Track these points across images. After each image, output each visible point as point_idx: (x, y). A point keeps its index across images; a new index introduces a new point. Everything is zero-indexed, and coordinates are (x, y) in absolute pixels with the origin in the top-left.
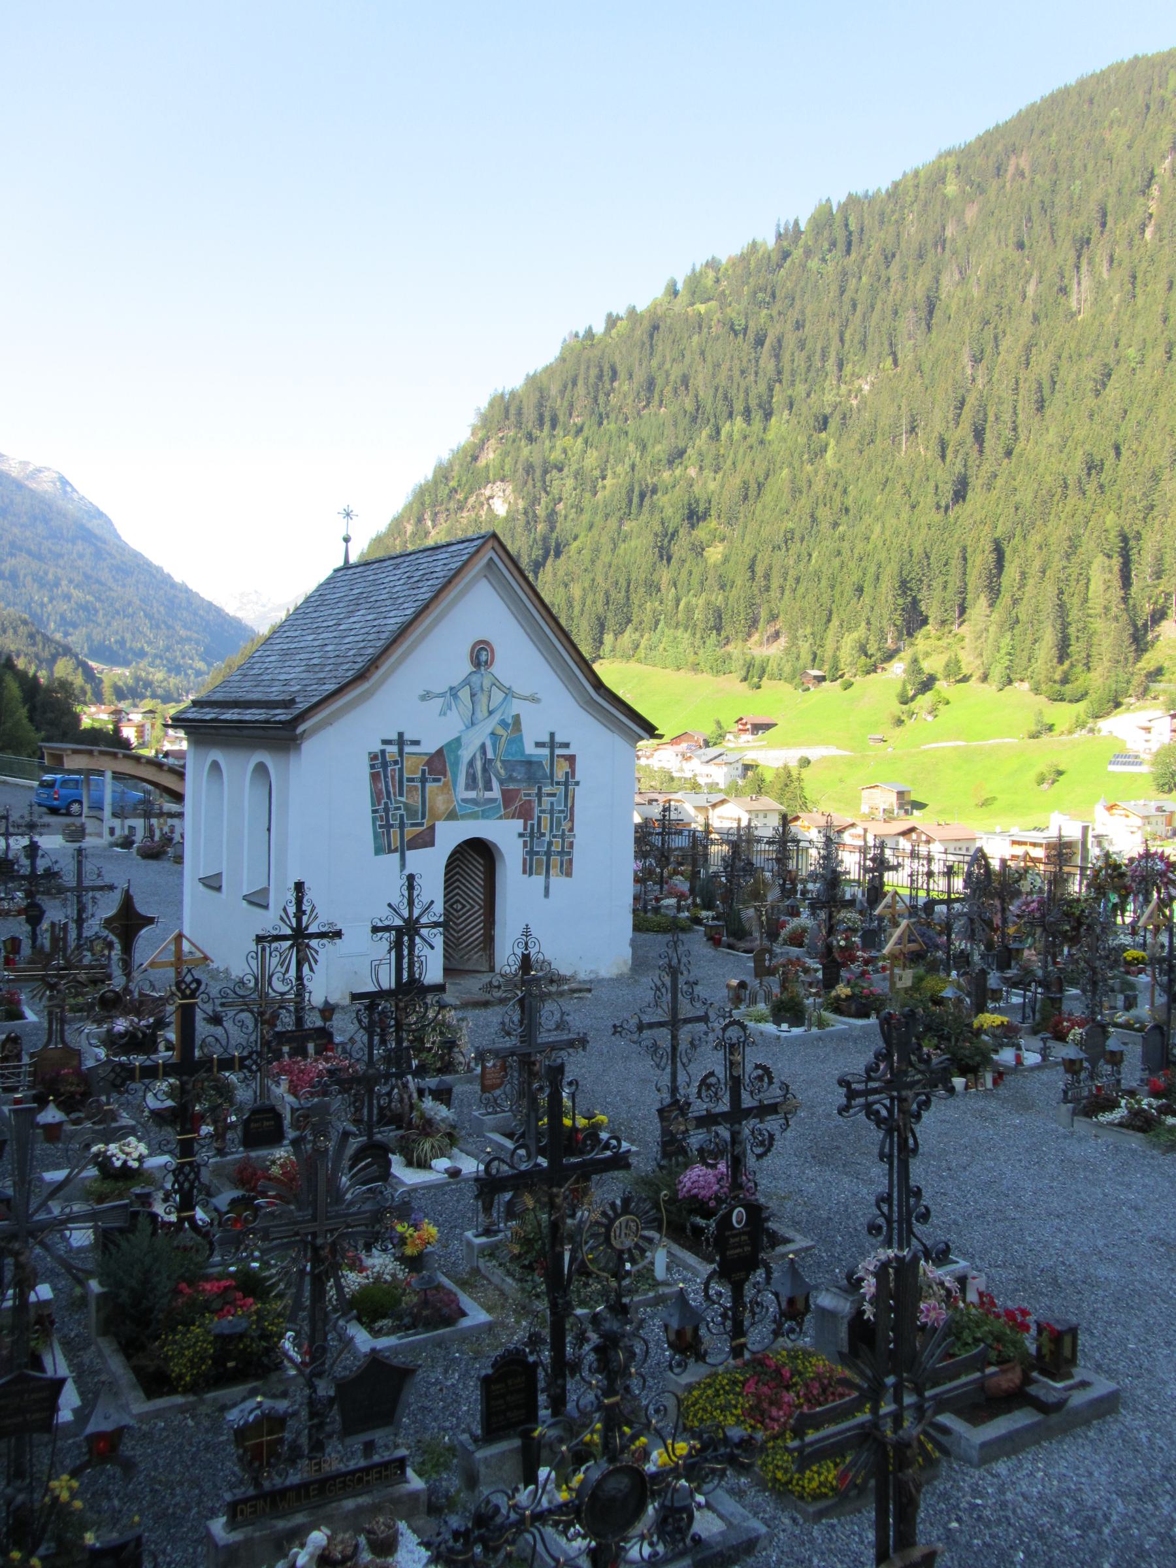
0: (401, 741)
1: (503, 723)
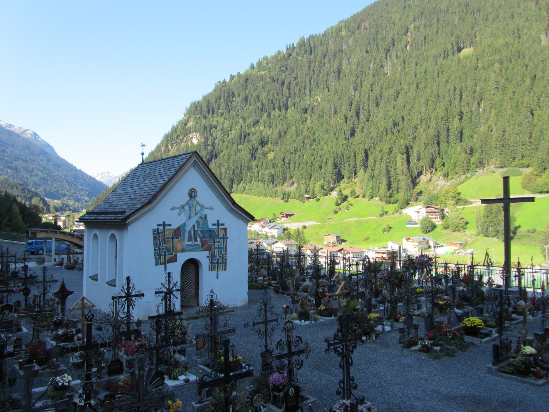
0: (164, 225)
1: (201, 217)
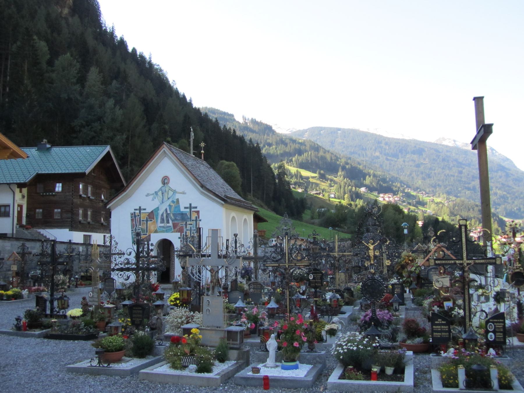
0: (140, 209)
1: (173, 202)
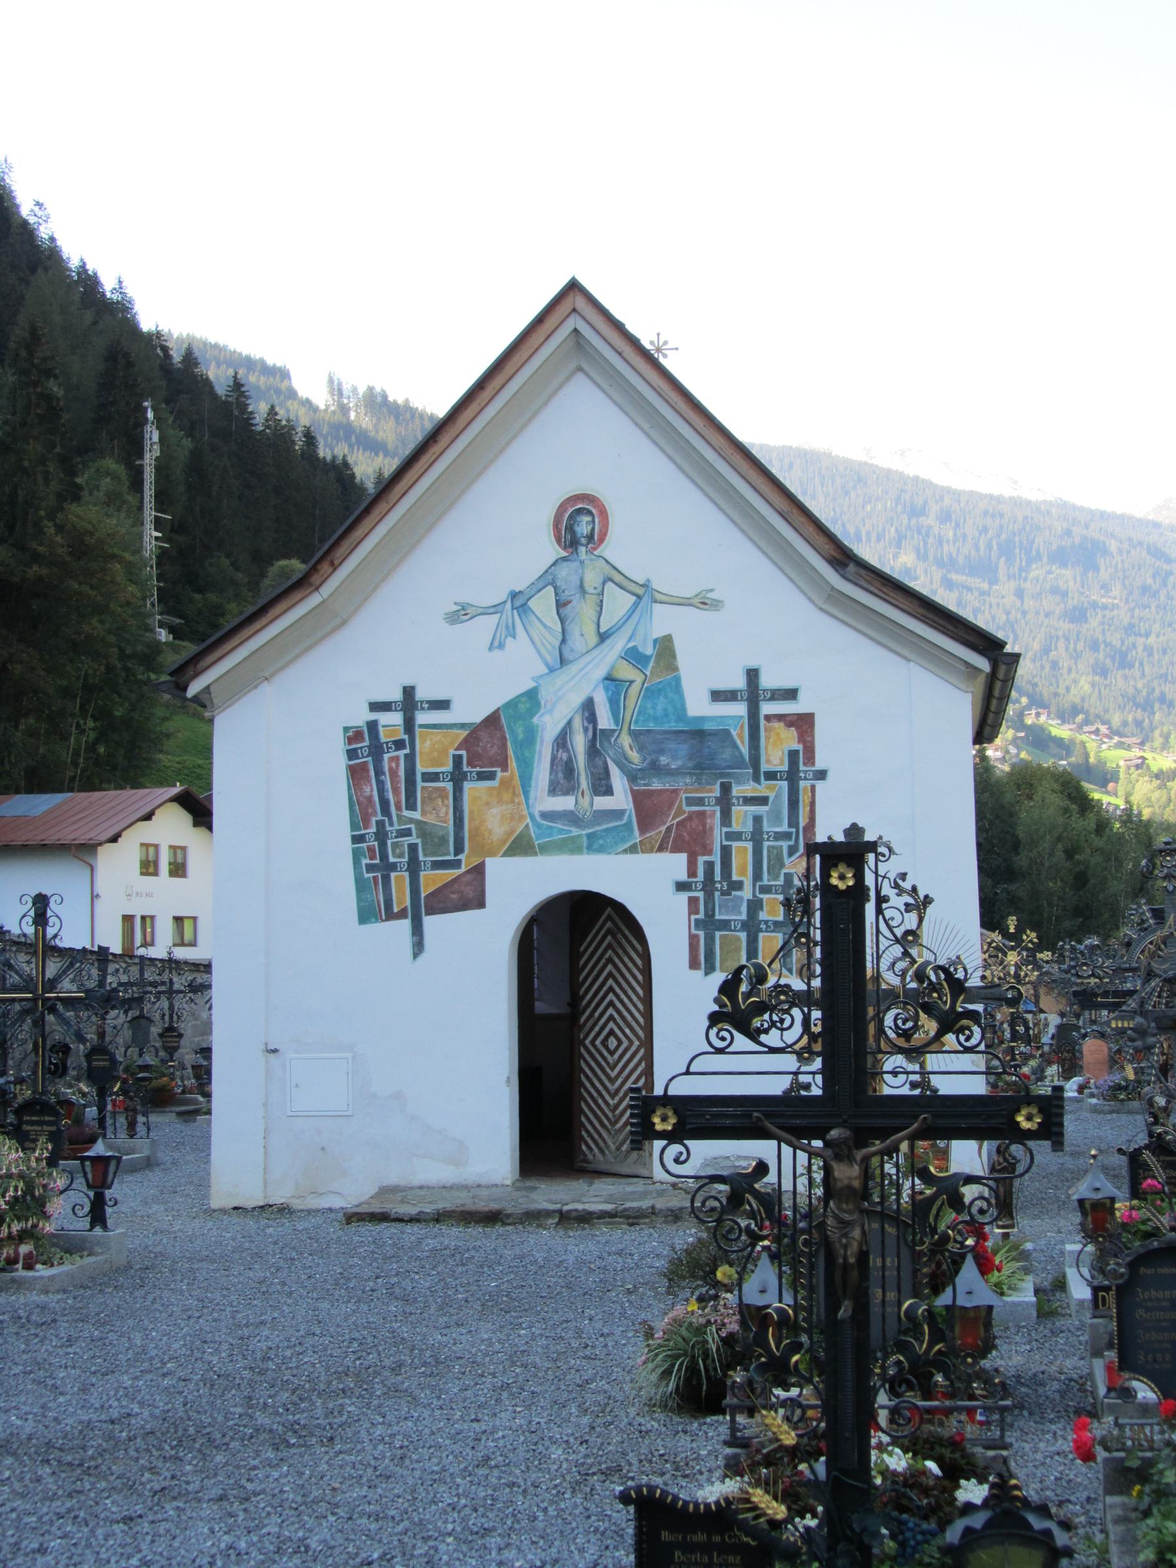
0: (409, 701)
1: (634, 657)
